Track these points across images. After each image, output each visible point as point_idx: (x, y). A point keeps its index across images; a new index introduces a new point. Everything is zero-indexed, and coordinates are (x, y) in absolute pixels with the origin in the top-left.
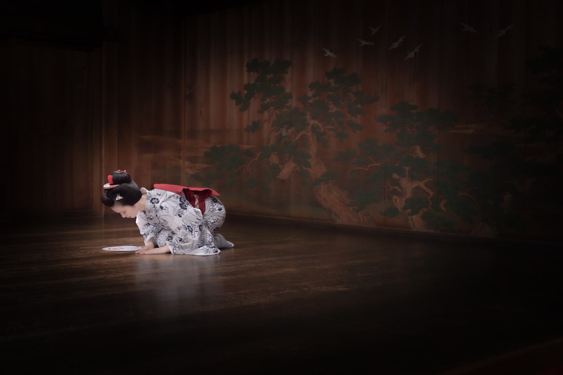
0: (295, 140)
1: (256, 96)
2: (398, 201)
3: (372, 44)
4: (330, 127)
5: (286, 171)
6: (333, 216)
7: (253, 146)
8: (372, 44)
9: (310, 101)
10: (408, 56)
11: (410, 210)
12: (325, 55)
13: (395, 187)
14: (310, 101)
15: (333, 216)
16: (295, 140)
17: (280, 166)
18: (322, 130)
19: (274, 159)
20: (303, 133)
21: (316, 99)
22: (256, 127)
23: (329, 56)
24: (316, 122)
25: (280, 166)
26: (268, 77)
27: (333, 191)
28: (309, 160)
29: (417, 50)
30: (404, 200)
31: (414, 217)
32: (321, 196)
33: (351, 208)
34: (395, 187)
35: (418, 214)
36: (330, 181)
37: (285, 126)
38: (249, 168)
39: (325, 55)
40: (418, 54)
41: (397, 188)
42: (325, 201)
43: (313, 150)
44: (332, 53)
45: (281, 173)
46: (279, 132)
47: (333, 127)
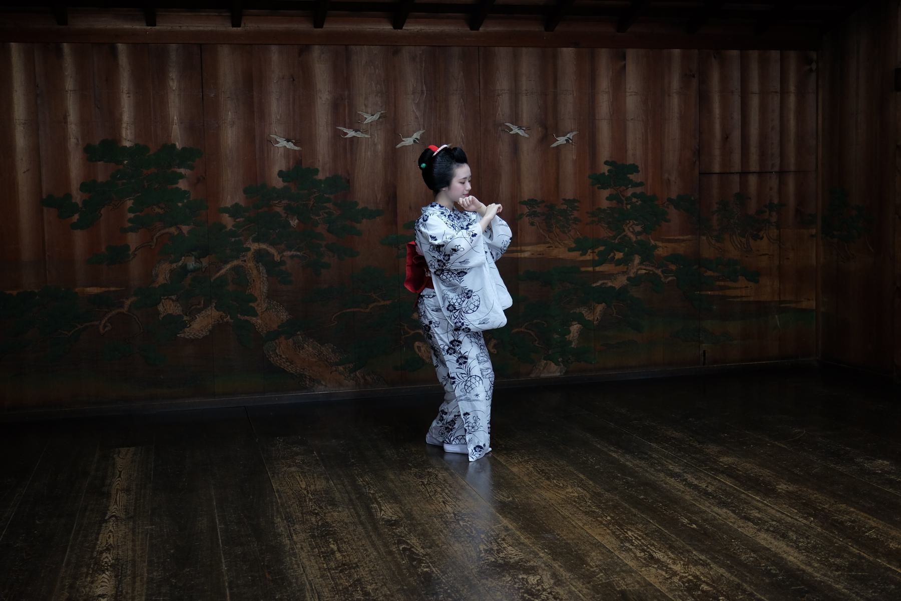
2: (423, 349)
4: (292, 252)
6: (308, 383)
8: (366, 136)
13: (418, 331)
15: (308, 383)
18: (277, 258)
24: (263, 246)
25: (185, 318)
28: (251, 304)
32: (281, 356)
33: (341, 368)
34: (418, 331)
36: (299, 333)
42: (289, 364)
44: (290, 143)
47: (299, 253)
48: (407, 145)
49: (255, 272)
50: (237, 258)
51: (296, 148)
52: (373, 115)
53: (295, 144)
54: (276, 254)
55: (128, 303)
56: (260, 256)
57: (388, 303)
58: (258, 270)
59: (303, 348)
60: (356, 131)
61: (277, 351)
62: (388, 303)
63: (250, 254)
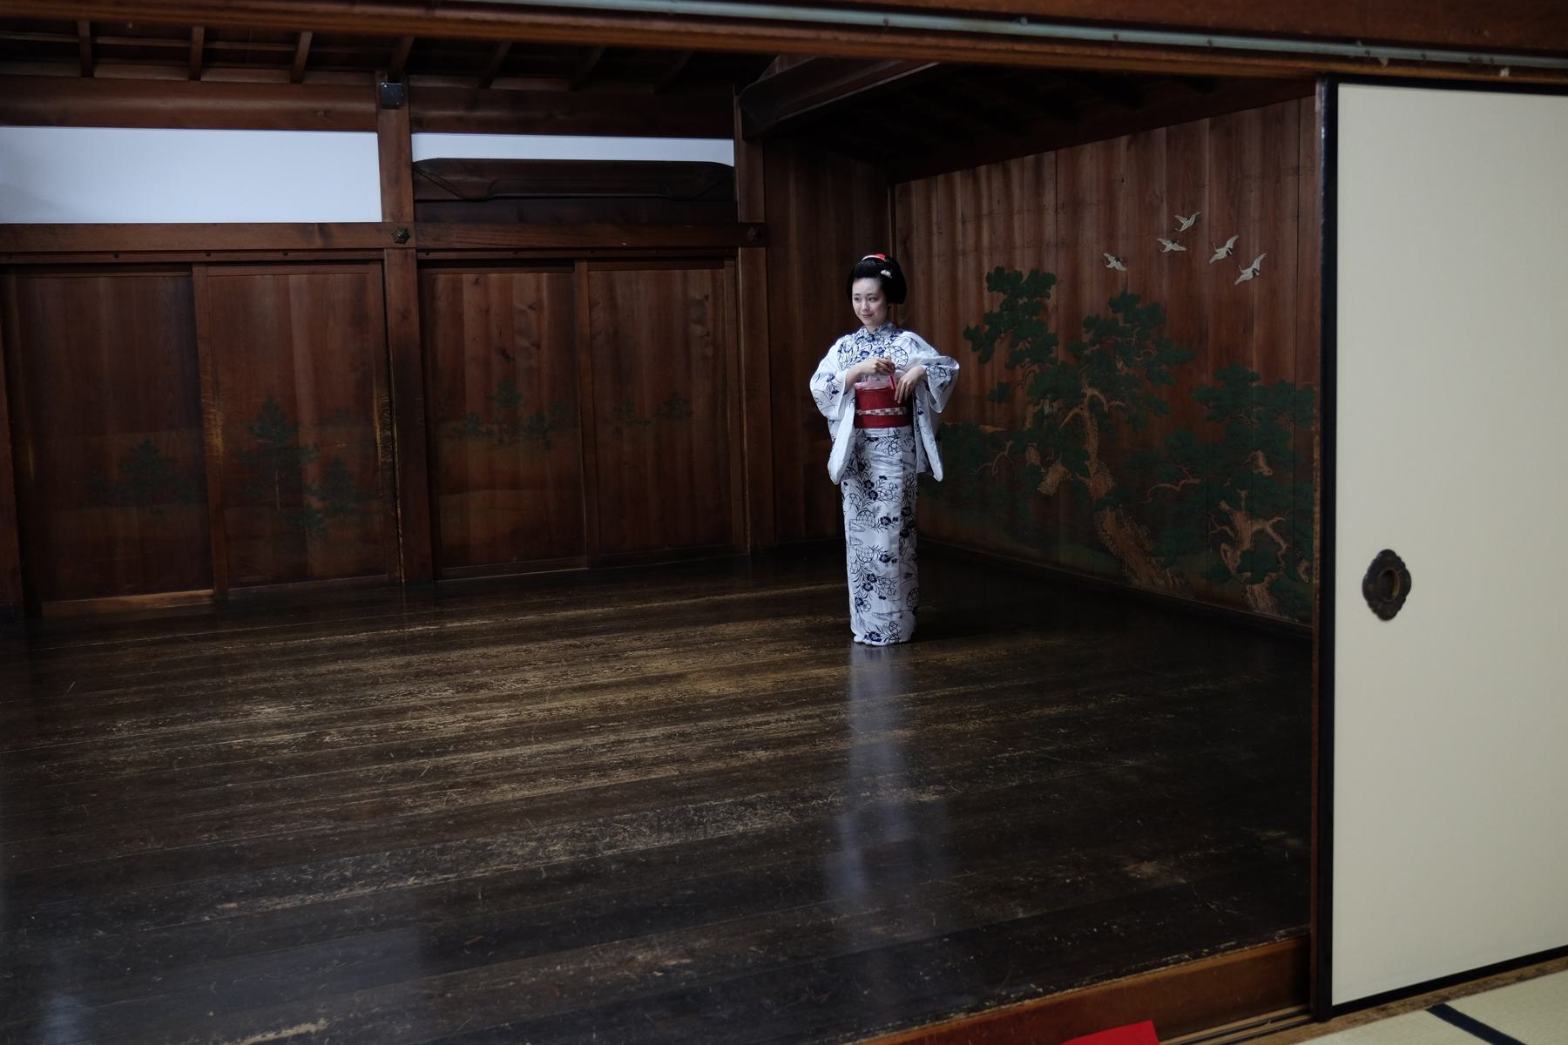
0: (1064, 423)
1: (1003, 335)
2: (1229, 554)
3: (1183, 249)
5: (1052, 479)
7: (1000, 429)
8: (1183, 249)
9: (1085, 352)
10: (1242, 276)
11: (1249, 574)
12: (1108, 266)
13: (1223, 528)
14: (1085, 352)
16: (1064, 423)
17: (1043, 470)
18: (1106, 409)
19: (1033, 456)
20: (1076, 410)
21: (1095, 348)
22: (1004, 394)
23: (1114, 268)
26: (1021, 302)
27: (1125, 524)
28: (1087, 463)
29: (1256, 265)
30: (1239, 553)
31: (1257, 587)
34: (1223, 528)
35: (1263, 584)
37: (1048, 395)
38: (995, 469)
39: (1108, 266)
40: (1258, 274)
41: (1227, 529)
43: (1092, 445)
45: (1043, 483)
46: (1039, 407)
48: (1220, 258)
49: (1089, 423)
50: (1077, 406)
51: (1124, 269)
52: (1189, 219)
53: (1123, 264)
54: (1104, 401)
55: (1008, 445)
56: (1094, 405)
57: (1196, 481)
58: (1092, 421)
59: (1124, 527)
60: (1173, 242)
61: (1104, 525)
62: (1196, 481)
63: (1086, 400)
